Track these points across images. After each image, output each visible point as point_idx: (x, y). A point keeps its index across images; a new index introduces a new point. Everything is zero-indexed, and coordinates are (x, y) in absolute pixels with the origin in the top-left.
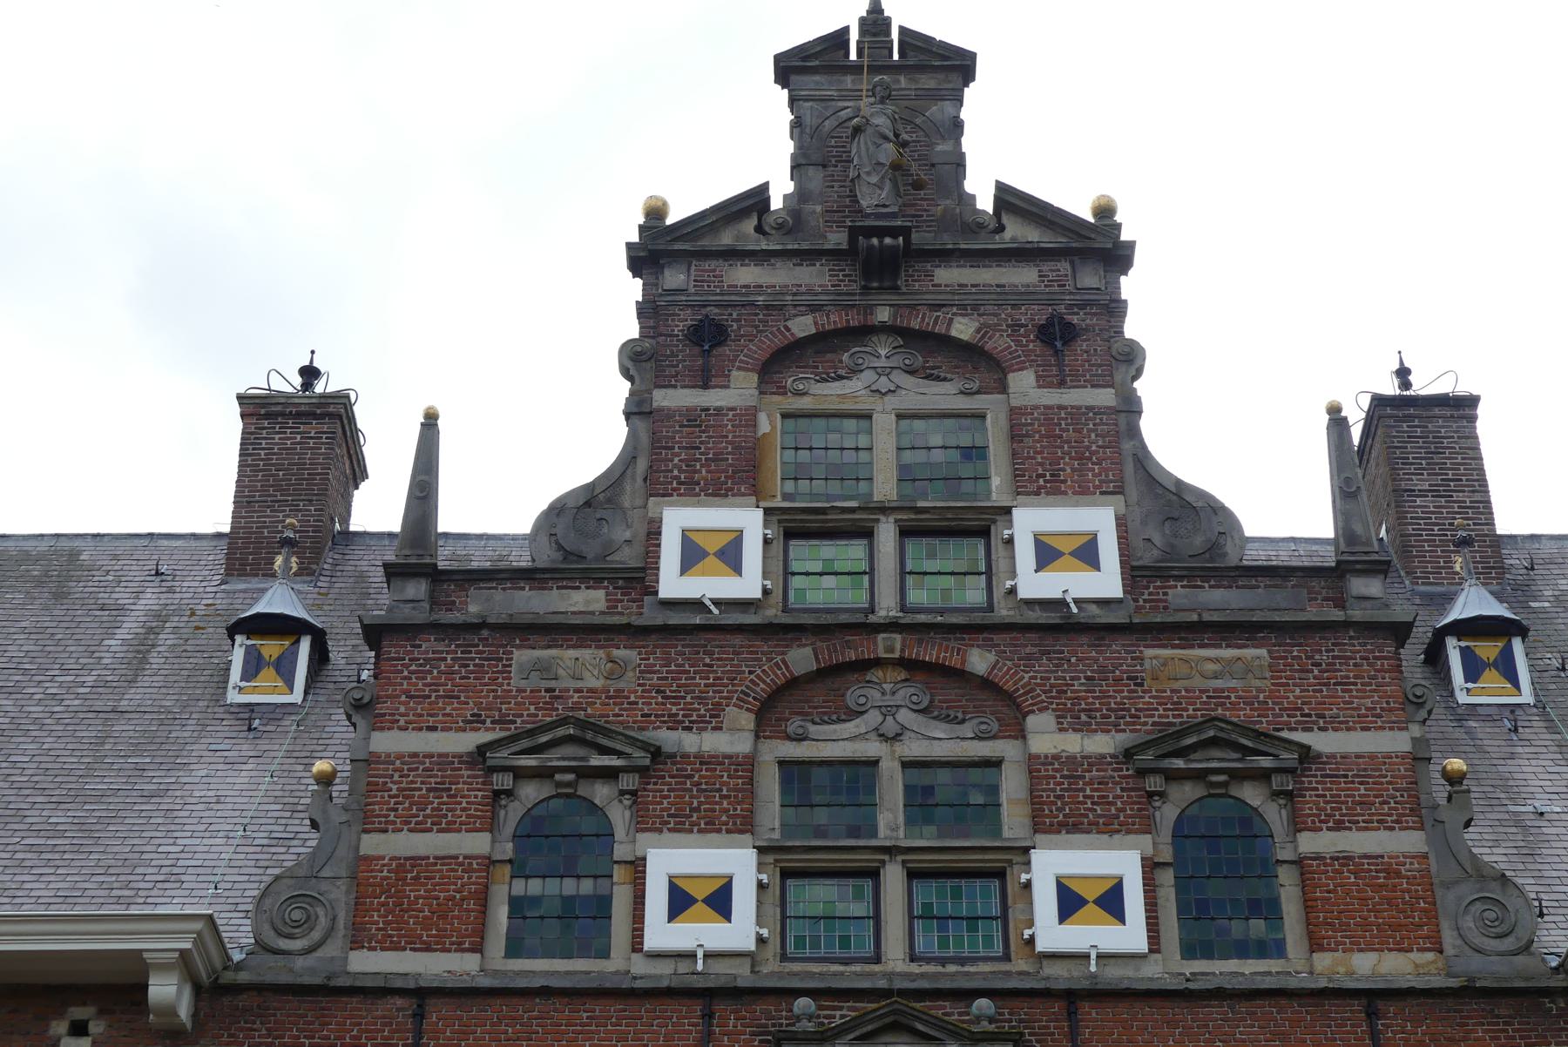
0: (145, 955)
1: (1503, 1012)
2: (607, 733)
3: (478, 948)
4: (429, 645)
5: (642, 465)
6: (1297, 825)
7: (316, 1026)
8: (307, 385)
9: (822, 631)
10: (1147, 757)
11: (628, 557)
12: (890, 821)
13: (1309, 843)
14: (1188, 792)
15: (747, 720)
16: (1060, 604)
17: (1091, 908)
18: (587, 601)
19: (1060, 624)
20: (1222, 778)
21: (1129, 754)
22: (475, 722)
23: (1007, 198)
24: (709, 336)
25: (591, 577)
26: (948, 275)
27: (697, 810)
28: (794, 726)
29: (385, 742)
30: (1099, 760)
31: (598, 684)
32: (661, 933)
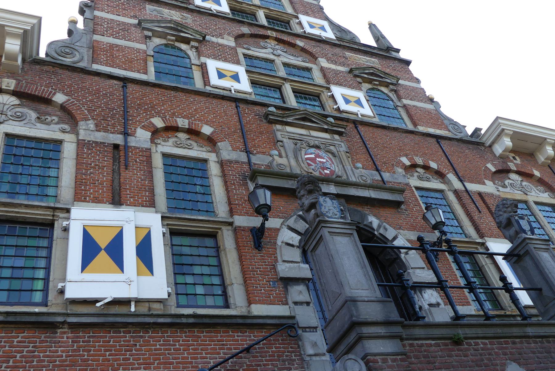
0: (6, 28)
1: (471, 147)
6: (399, 98)
7: (80, 82)
10: (357, 72)
15: (233, 39)
16: (320, 36)
17: (353, 103)
20: (377, 83)
21: (351, 71)
27: (221, 55)
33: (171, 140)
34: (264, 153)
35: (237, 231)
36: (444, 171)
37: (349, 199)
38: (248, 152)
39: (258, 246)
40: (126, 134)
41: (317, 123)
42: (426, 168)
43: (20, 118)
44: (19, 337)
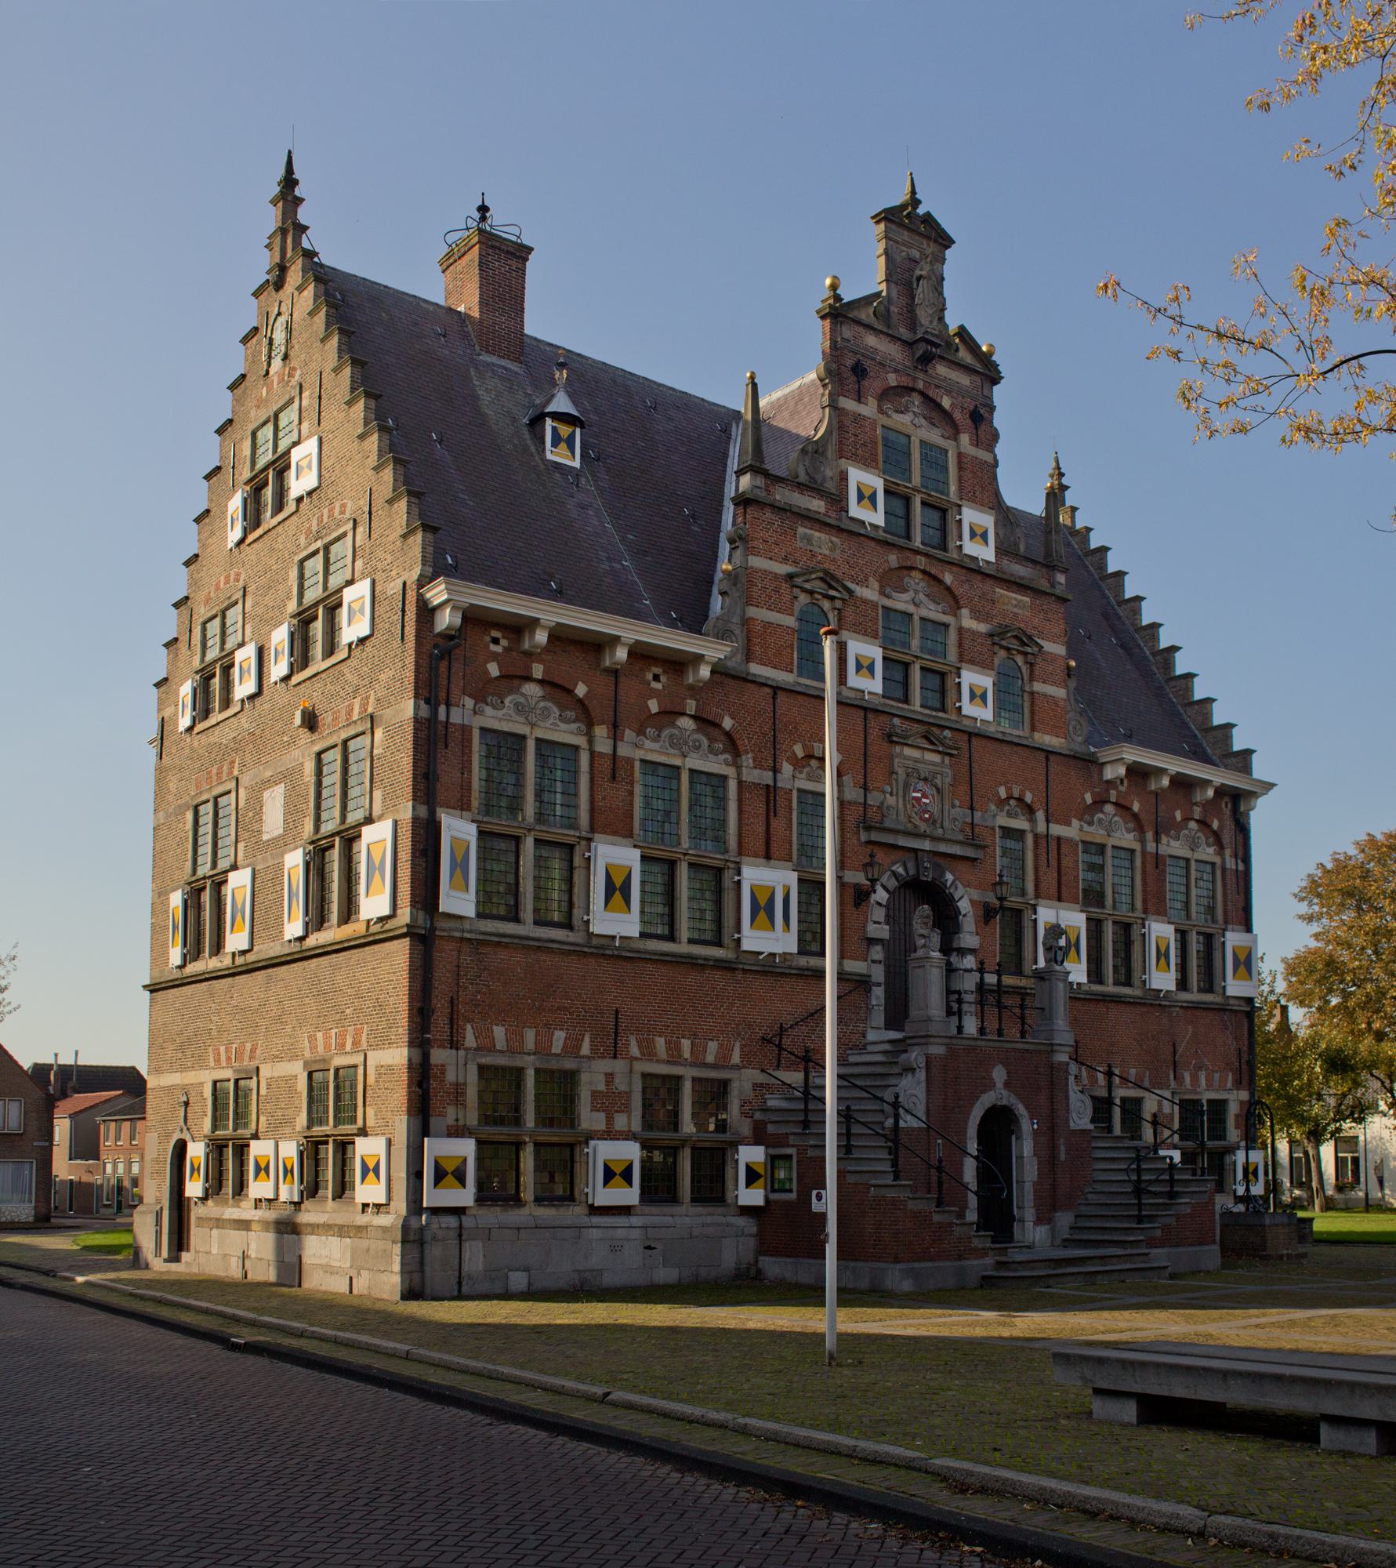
2: (838, 581)
3: (791, 672)
4: (768, 514)
6: (1032, 679)
13: (1038, 687)
14: (1002, 653)
15: (876, 585)
18: (817, 505)
19: (971, 568)
21: (991, 635)
22: (785, 560)
28: (888, 590)
29: (755, 562)
30: (981, 634)
31: (827, 552)
33: (806, 770)
34: (877, 789)
36: (1036, 806)
37: (936, 853)
38: (865, 788)
40: (775, 770)
41: (932, 743)
42: (1020, 800)
43: (697, 748)
44: (718, 975)
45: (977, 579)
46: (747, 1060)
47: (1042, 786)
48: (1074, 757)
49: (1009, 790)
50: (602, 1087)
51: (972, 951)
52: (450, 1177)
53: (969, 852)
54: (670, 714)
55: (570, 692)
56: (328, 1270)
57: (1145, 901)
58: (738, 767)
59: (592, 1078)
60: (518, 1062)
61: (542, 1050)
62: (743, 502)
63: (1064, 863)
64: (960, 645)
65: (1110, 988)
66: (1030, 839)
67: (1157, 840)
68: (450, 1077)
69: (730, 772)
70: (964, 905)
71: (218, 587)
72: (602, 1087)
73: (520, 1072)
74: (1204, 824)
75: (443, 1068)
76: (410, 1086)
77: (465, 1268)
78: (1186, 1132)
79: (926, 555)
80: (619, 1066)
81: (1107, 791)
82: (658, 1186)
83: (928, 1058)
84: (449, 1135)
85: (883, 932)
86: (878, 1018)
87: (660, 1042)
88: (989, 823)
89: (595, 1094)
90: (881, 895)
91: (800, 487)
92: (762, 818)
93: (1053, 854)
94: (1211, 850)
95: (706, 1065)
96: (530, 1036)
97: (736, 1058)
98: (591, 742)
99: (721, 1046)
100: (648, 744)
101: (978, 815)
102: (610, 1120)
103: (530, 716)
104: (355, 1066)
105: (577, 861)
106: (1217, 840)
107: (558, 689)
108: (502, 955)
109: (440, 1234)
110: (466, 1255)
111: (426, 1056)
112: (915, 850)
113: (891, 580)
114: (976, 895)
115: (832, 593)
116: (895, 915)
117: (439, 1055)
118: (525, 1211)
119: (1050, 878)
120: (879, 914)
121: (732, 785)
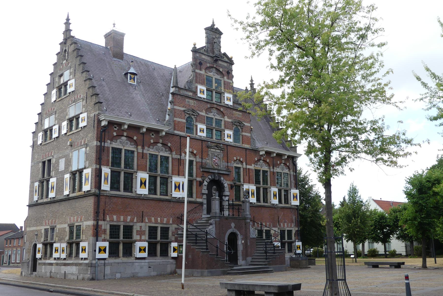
4: (179, 97)
5: (195, 78)
6: (242, 132)
8: (114, 26)
9: (210, 103)
11: (194, 90)
12: (214, 125)
13: (244, 134)
14: (235, 126)
15: (205, 112)
18: (190, 94)
22: (183, 107)
23: (225, 54)
24: (200, 64)
25: (191, 91)
26: (220, 62)
28: (207, 113)
30: (230, 122)
32: (199, 134)
35: (197, 181)
39: (200, 186)
40: (181, 155)
42: (239, 160)
45: (229, 110)
46: (174, 222)
47: (245, 157)
48: (252, 150)
49: (237, 158)
50: (139, 229)
51: (228, 196)
52: (102, 251)
53: (227, 173)
54: (156, 143)
55: (132, 138)
56: (72, 274)
57: (271, 183)
58: (172, 155)
59: (136, 228)
60: (119, 224)
61: (125, 221)
62: (173, 94)
63: (250, 174)
64: (225, 124)
65: (262, 204)
66: (242, 169)
67: (273, 168)
68: (103, 228)
69: (170, 156)
70: (226, 185)
71: (49, 111)
72: (139, 229)
73: (119, 226)
74: (285, 164)
75: (101, 226)
76: (93, 230)
77: (106, 272)
78: (282, 237)
79: (216, 104)
80: (143, 224)
81: (261, 157)
82: (152, 252)
83: (216, 221)
84: (102, 241)
85: (206, 192)
86: (205, 212)
87: (153, 219)
88: (232, 166)
89: (137, 231)
90: (205, 183)
91: (186, 90)
92: (177, 166)
93: (248, 173)
94: (287, 170)
95: (164, 224)
96: (122, 218)
97: (171, 222)
98: (137, 150)
99: (167, 219)
100: (151, 150)
101: (229, 164)
102: (141, 237)
103: (123, 144)
104: (81, 225)
105: (134, 177)
106: (289, 168)
107: (130, 138)
108: (116, 199)
109: (100, 265)
110: (106, 270)
111: (98, 223)
112: (214, 173)
113: (208, 110)
114: (229, 182)
115: (194, 114)
116: (209, 187)
117: (101, 223)
118: (120, 259)
119: (247, 178)
120: (205, 188)
121: (170, 159)
